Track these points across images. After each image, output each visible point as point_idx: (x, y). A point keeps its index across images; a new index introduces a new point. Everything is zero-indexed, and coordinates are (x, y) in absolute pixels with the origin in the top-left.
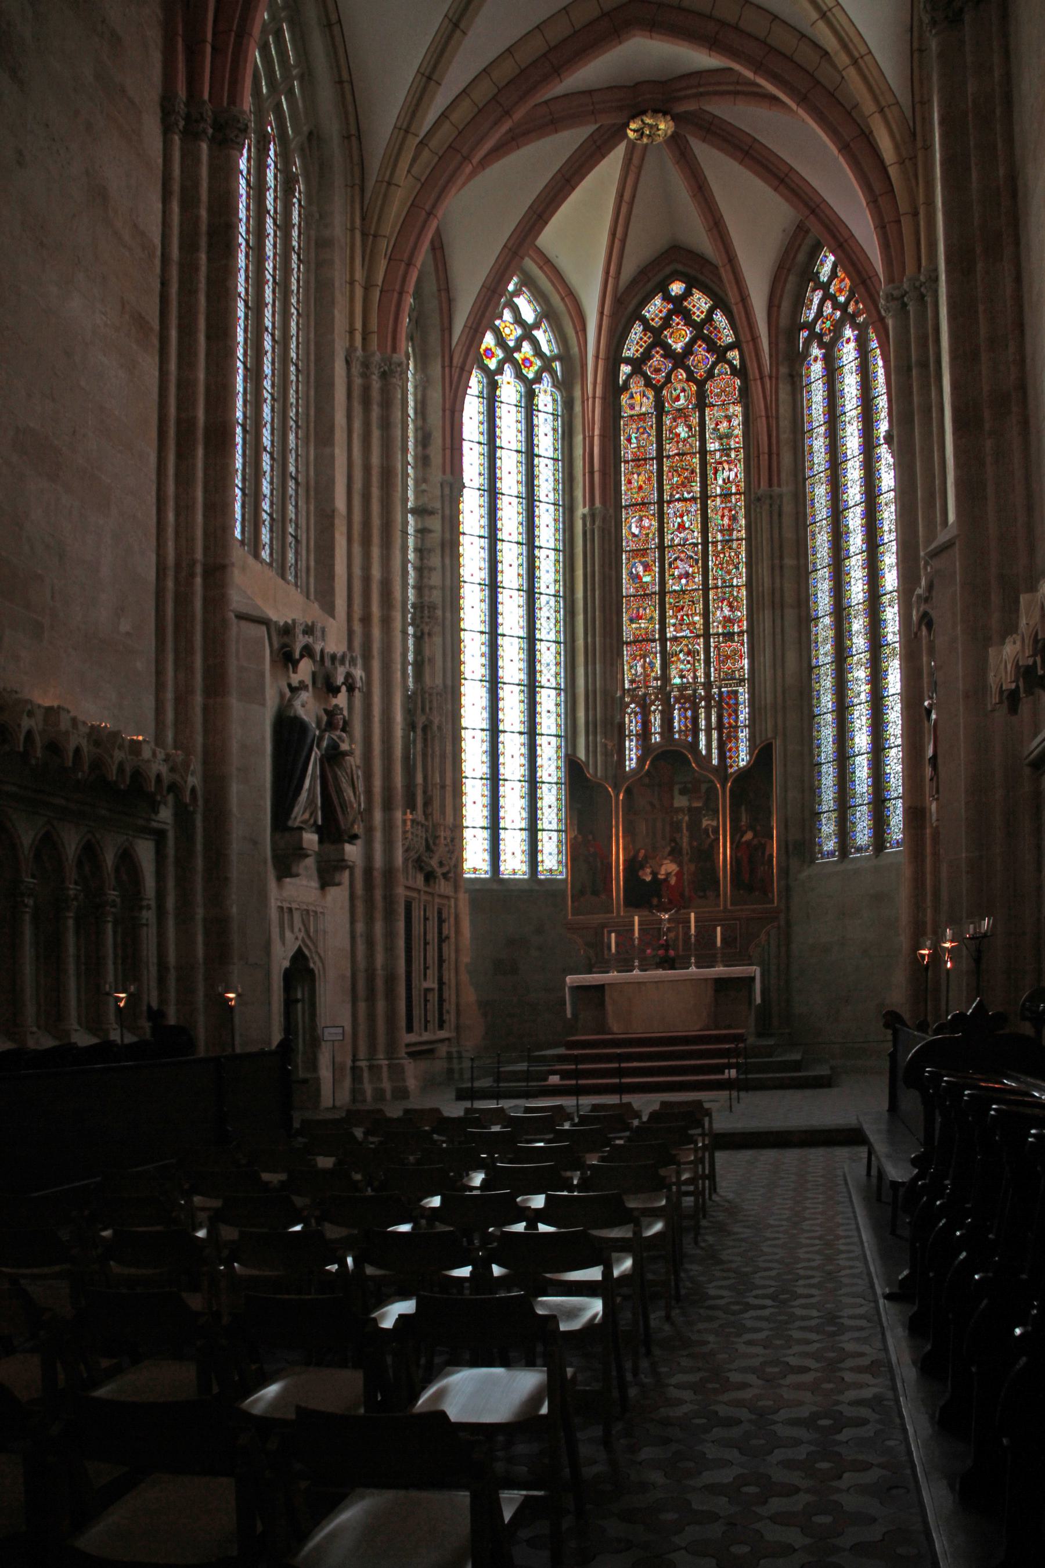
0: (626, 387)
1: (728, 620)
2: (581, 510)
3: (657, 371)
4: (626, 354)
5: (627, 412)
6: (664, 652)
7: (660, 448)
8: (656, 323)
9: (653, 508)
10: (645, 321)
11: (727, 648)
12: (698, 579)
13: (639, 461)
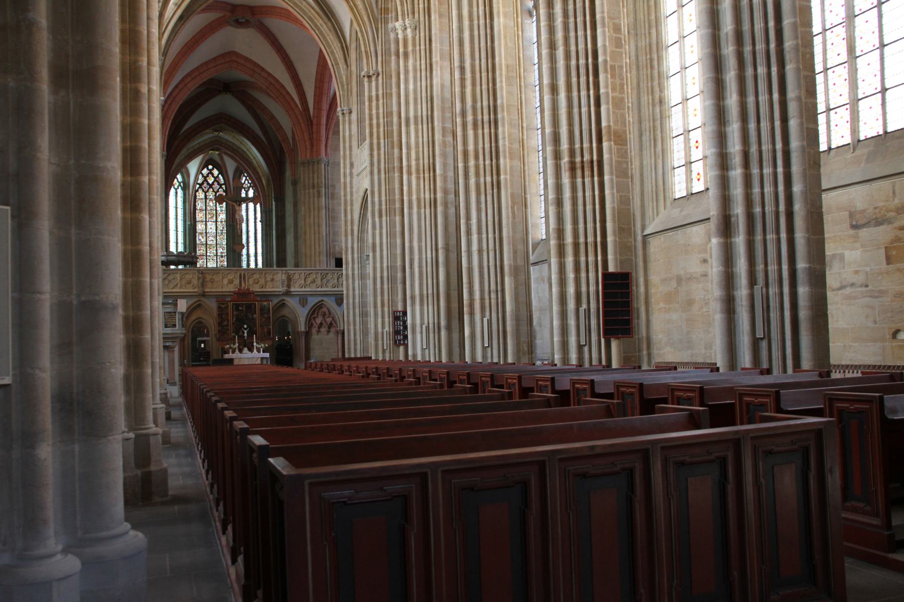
0: (197, 191)
1: (222, 253)
2: (188, 223)
3: (205, 188)
4: (198, 182)
5: (198, 197)
6: (207, 259)
7: (206, 208)
8: (205, 175)
9: (204, 223)
10: (202, 174)
11: (222, 259)
12: (215, 241)
13: (201, 210)
